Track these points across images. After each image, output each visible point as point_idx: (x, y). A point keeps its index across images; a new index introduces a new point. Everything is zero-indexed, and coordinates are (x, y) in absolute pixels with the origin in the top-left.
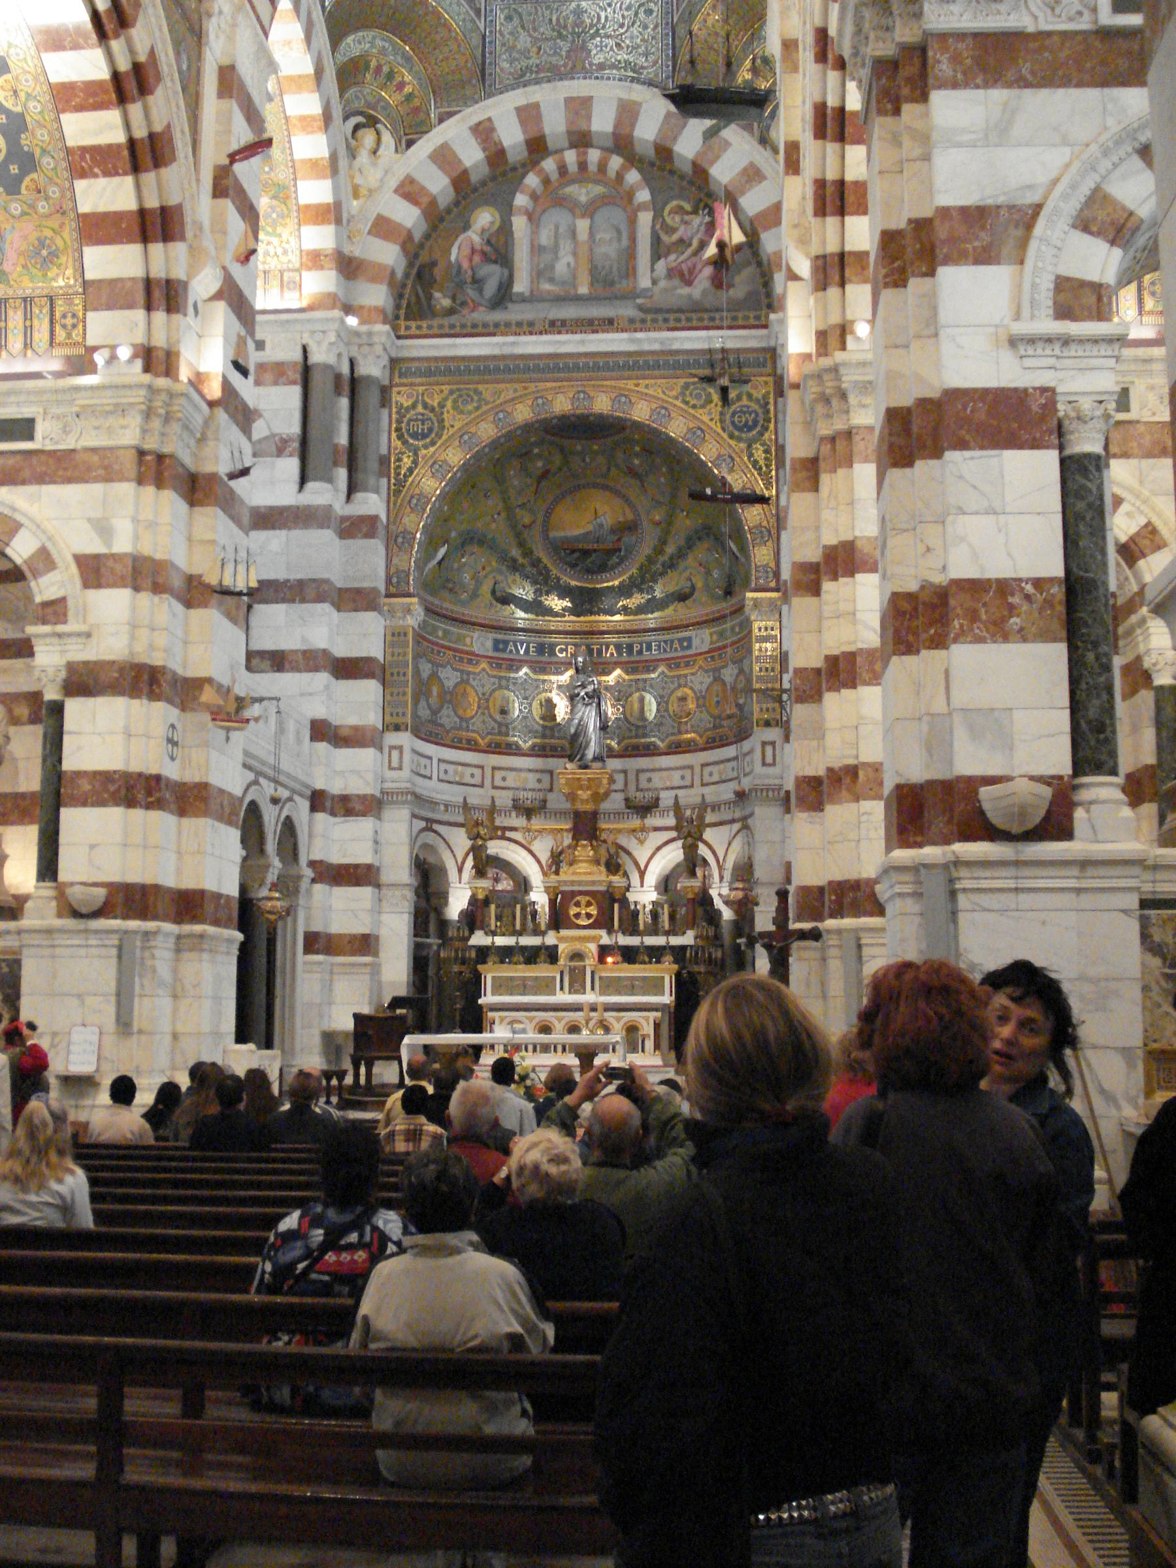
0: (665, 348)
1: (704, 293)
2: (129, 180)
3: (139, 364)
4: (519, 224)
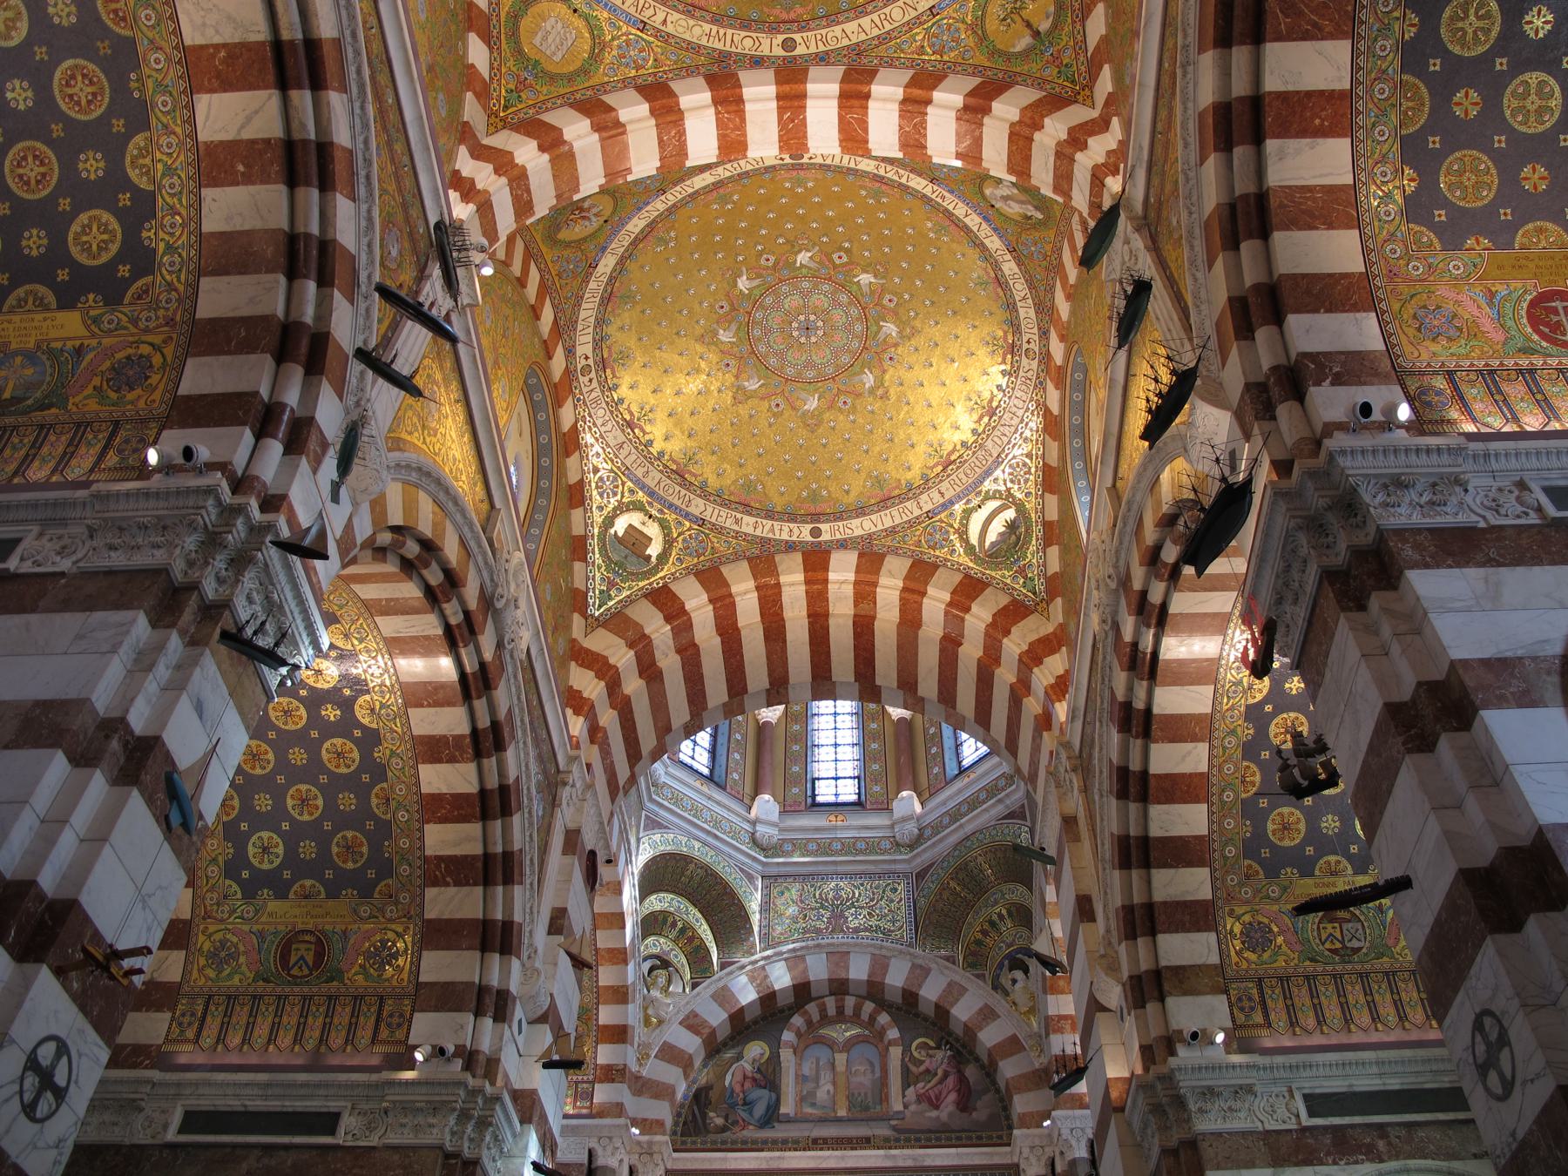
0: (918, 1164)
1: (950, 1115)
2: (479, 890)
3: (459, 1063)
4: (786, 1055)
